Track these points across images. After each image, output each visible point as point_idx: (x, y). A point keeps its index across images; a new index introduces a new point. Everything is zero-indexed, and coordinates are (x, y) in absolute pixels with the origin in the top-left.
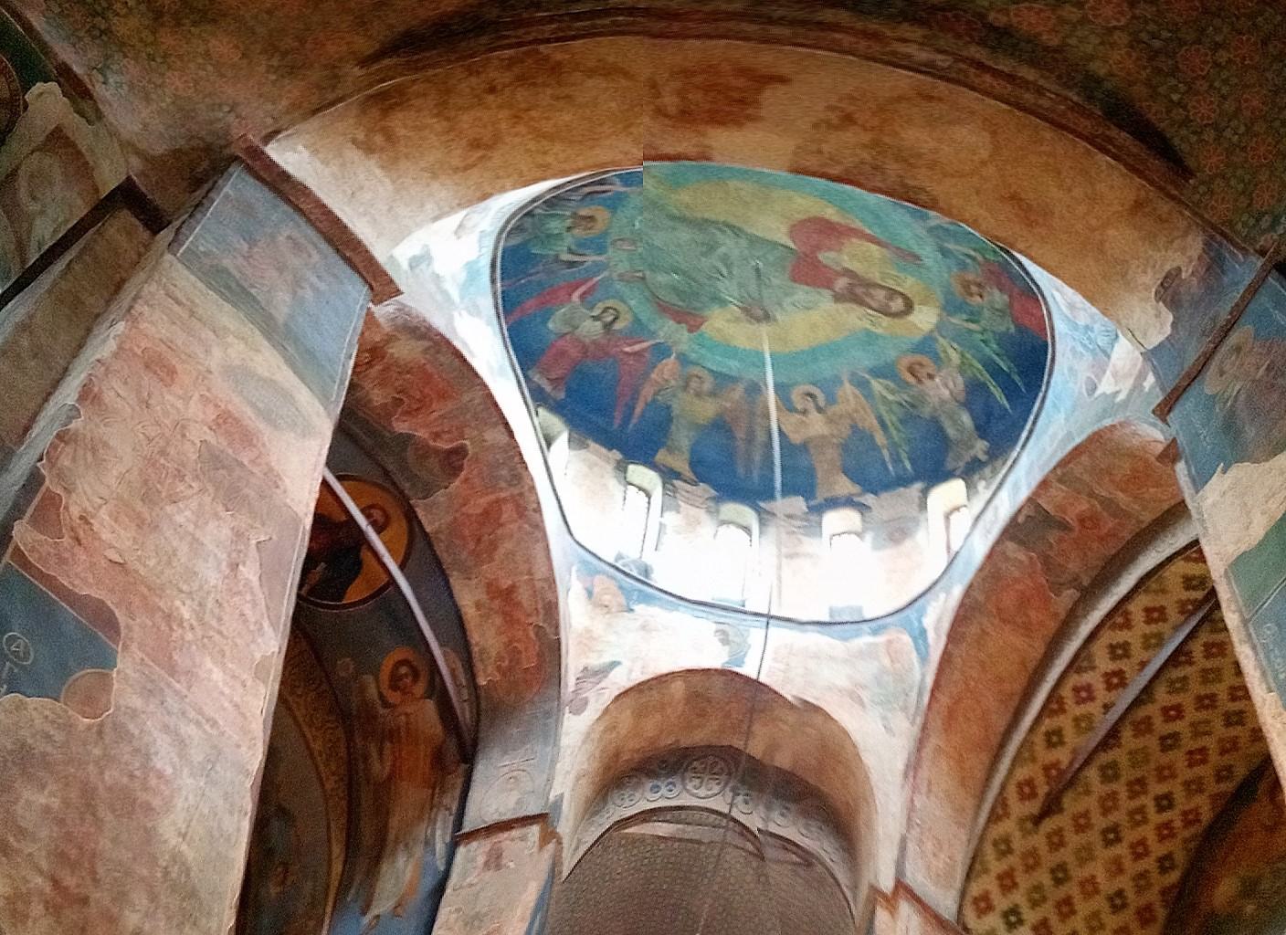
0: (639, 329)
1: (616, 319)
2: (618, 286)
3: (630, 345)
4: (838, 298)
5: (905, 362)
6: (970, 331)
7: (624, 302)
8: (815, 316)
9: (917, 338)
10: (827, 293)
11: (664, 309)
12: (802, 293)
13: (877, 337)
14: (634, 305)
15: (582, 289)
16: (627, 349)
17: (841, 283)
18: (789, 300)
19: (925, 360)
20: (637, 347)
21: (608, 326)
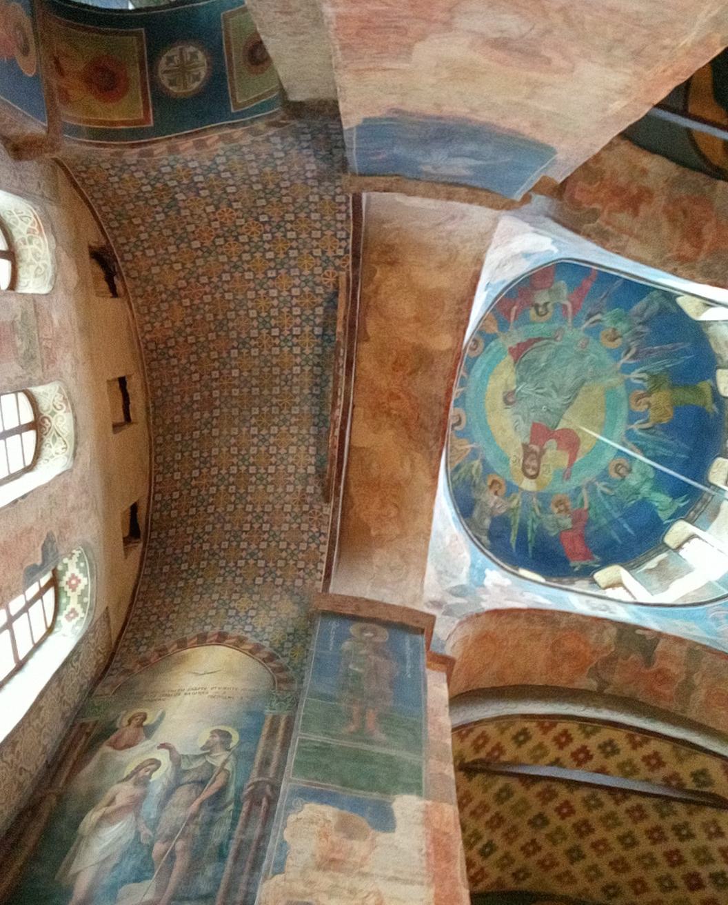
0: (523, 320)
1: (538, 313)
2: (556, 325)
3: (517, 311)
4: (525, 446)
5: (497, 478)
6: (534, 510)
7: (548, 322)
8: (510, 432)
9: (515, 483)
10: (527, 440)
11: (530, 343)
12: (525, 427)
13: (508, 464)
14: (540, 327)
15: (570, 310)
16: (515, 308)
17: (535, 448)
18: (520, 418)
19: (503, 490)
20: (513, 313)
21: (537, 306)
